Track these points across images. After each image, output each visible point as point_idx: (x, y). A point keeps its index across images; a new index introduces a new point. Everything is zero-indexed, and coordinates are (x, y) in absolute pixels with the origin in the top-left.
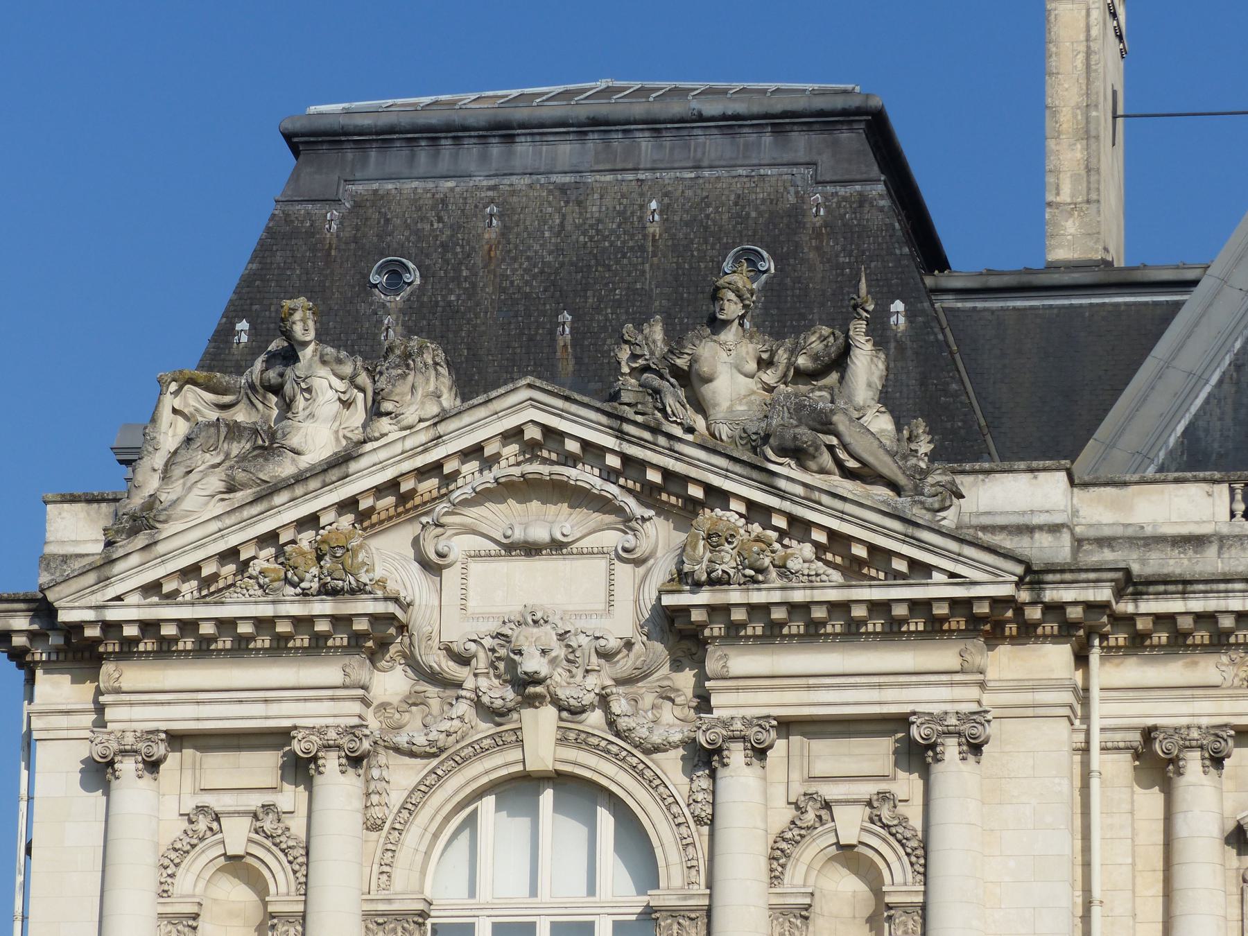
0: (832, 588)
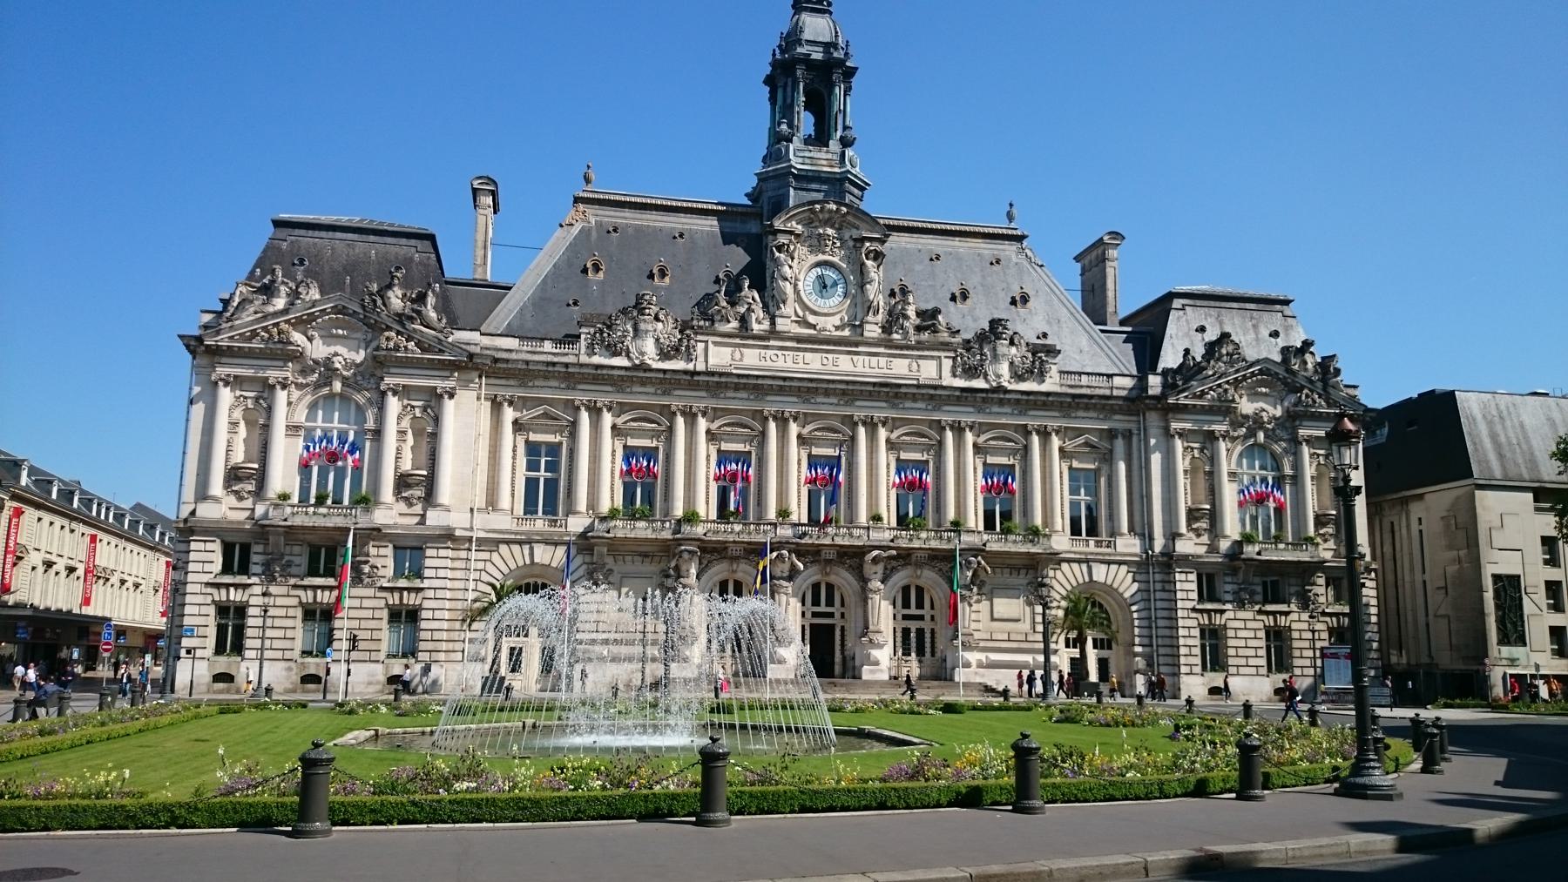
0: (418, 354)
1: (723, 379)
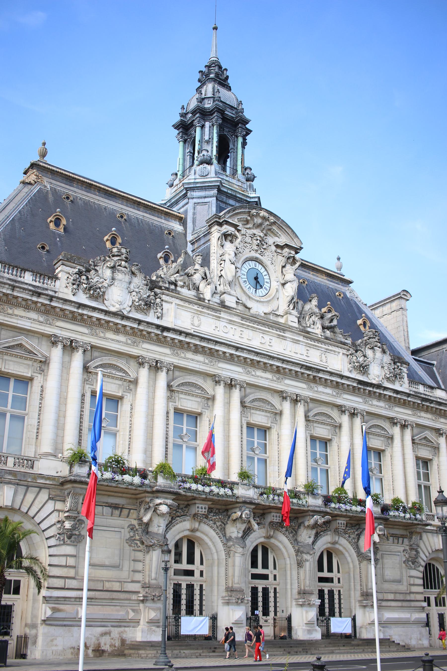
1: (188, 340)
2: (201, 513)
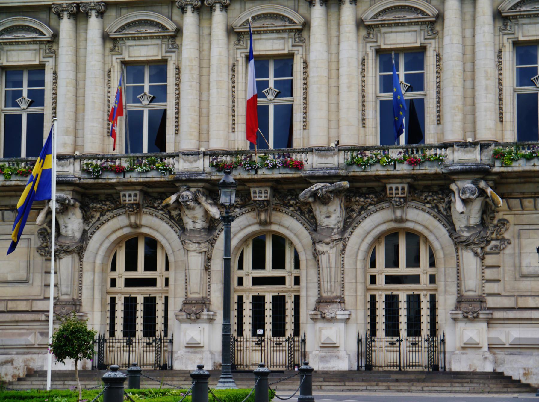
2: (130, 202)
